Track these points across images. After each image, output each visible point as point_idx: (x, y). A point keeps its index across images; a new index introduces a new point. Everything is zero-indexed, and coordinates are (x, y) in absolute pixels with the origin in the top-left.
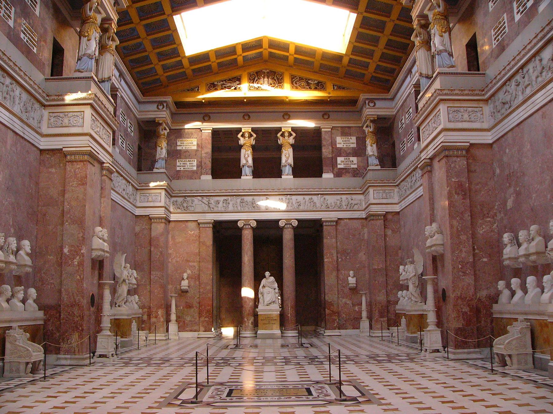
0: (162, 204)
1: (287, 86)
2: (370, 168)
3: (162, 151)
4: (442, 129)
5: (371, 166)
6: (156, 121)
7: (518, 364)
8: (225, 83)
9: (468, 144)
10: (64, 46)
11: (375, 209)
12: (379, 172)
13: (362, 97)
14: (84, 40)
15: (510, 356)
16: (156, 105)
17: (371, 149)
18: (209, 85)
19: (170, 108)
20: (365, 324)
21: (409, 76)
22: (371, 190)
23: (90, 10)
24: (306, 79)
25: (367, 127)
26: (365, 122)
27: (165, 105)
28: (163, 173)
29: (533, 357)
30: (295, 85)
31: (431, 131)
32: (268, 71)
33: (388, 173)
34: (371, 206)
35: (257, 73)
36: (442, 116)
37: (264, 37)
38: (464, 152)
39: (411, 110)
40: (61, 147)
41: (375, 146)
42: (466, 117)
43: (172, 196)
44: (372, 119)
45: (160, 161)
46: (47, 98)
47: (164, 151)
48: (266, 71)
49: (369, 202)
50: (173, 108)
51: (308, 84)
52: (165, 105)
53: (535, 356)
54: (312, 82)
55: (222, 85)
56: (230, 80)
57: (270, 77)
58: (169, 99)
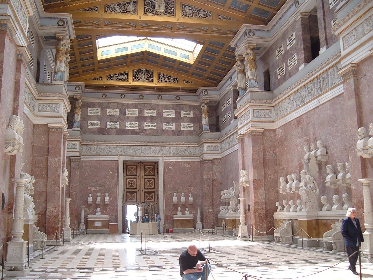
0: (78, 150)
1: (156, 79)
2: (204, 131)
3: (78, 117)
4: (251, 121)
5: (204, 130)
6: (75, 98)
7: (286, 242)
8: (118, 76)
9: (263, 129)
10: (41, 62)
11: (205, 156)
12: (210, 134)
13: (202, 88)
14: (58, 62)
15: (281, 237)
16: (74, 87)
17: (205, 121)
18: (108, 76)
19: (82, 90)
20: (199, 225)
21: (230, 79)
22: (205, 145)
23: (62, 45)
24: (167, 76)
25: (203, 106)
26: (203, 103)
27: (80, 87)
28: (79, 130)
29: (293, 238)
30: (161, 79)
31: (244, 121)
32: (144, 69)
33: (215, 135)
34: (204, 154)
35: (138, 70)
36: (250, 114)
37: (146, 52)
38: (261, 134)
39: (230, 100)
40: (46, 124)
41: (207, 118)
42: (263, 115)
43: (81, 145)
44: (206, 102)
45: (77, 123)
46: (38, 95)
47: (79, 117)
48: (143, 70)
49: (203, 152)
50: (83, 88)
51: (169, 79)
52: (80, 87)
53: (294, 237)
54: (171, 78)
55: (116, 77)
56: (121, 74)
57: (146, 74)
58: (82, 84)
